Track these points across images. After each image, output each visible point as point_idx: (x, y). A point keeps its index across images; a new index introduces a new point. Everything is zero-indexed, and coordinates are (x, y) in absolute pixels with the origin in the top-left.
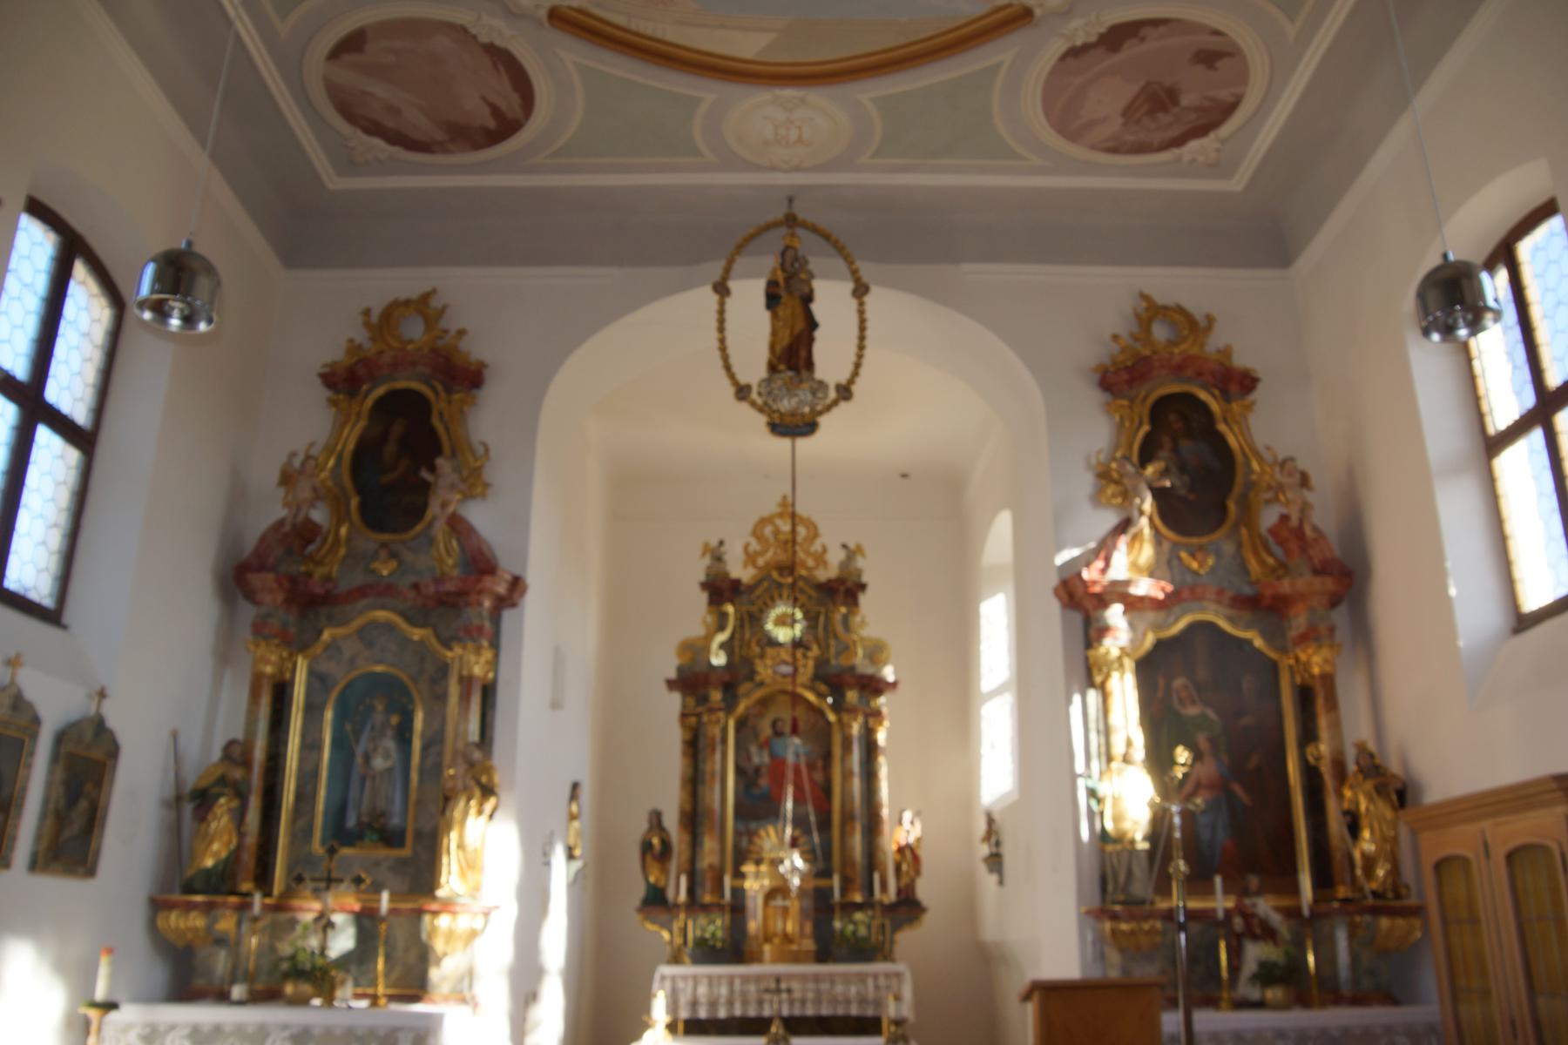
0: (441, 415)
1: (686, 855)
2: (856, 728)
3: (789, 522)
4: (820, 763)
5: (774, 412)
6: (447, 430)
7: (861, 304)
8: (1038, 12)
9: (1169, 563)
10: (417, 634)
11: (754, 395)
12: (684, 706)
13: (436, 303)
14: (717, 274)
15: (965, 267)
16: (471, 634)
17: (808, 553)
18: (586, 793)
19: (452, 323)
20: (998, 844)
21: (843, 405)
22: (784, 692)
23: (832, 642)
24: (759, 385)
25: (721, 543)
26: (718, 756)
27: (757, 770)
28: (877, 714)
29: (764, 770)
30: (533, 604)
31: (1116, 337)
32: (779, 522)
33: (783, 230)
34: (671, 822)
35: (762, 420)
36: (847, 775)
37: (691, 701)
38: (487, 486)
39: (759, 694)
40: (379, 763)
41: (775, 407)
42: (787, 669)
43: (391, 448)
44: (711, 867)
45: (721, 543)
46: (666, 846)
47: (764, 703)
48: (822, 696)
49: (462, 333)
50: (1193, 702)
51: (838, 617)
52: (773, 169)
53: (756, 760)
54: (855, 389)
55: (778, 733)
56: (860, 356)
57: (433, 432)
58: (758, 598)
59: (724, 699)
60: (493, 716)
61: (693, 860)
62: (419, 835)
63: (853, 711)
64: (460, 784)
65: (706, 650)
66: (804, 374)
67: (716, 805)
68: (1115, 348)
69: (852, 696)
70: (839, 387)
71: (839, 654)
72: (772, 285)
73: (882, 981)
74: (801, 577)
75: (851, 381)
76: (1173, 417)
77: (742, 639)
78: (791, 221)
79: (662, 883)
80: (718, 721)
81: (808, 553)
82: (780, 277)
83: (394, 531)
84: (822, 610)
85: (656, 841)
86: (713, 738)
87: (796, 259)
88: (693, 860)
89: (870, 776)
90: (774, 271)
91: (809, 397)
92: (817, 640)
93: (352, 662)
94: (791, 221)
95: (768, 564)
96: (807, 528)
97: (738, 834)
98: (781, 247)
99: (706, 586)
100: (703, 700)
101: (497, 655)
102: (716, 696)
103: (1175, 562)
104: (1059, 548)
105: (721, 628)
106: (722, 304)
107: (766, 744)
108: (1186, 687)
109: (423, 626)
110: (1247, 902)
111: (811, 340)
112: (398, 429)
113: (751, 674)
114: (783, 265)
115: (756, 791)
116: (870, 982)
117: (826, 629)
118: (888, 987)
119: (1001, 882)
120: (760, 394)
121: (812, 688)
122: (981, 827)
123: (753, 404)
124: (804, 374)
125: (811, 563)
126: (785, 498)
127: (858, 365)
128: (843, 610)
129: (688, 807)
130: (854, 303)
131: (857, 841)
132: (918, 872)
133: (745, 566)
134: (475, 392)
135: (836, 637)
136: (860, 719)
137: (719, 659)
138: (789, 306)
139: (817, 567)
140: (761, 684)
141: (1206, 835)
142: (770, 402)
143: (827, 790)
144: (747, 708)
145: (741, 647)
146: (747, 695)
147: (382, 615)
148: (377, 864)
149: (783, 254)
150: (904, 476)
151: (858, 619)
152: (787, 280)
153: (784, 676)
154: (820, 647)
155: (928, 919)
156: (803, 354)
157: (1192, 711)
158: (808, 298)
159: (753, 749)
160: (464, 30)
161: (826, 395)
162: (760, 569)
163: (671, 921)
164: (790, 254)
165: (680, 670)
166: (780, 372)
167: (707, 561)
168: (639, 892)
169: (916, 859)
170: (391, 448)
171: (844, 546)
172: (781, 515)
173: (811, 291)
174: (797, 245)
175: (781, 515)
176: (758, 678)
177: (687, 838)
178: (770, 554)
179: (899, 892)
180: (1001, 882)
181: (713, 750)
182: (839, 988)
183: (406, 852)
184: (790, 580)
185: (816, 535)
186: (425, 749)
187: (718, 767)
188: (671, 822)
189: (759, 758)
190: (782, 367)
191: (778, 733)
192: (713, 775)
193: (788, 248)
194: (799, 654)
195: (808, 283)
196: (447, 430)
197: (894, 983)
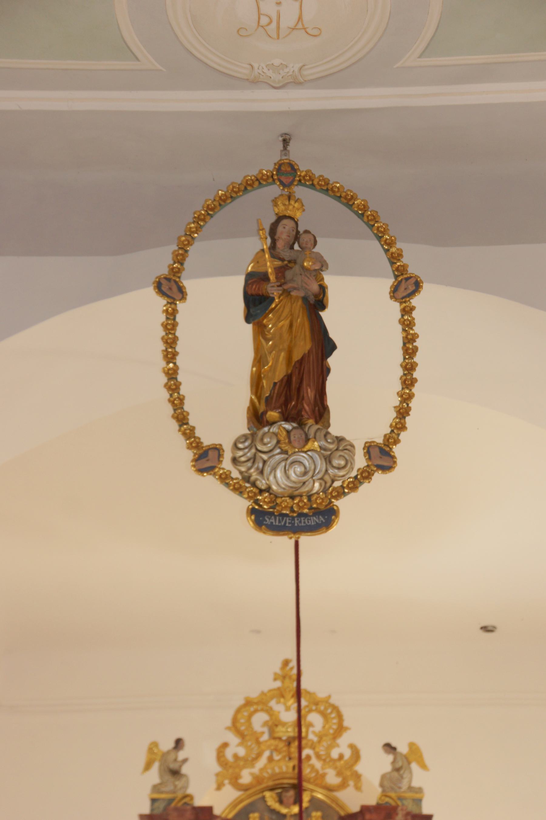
3: (292, 703)
5: (261, 491)
7: (407, 311)
11: (227, 464)
17: (326, 760)
21: (378, 476)
24: (235, 447)
25: (179, 743)
32: (277, 706)
33: (275, 190)
35: (244, 504)
41: (262, 484)
45: (179, 743)
54: (397, 450)
66: (312, 426)
70: (369, 448)
74: (316, 803)
81: (326, 760)
82: (270, 268)
87: (297, 237)
90: (258, 258)
91: (321, 465)
95: (258, 780)
96: (324, 714)
111: (325, 371)
114: (273, 247)
120: (235, 461)
123: (225, 479)
124: (312, 426)
125: (332, 778)
126: (286, 663)
130: (396, 308)
133: (219, 787)
139: (343, 785)
142: (254, 475)
150: (486, 629)
152: (281, 271)
156: (310, 393)
161: (349, 463)
162: (245, 788)
166: (272, 424)
171: (389, 748)
172: (280, 694)
173: (323, 289)
174: (298, 215)
175: (280, 694)
178: (262, 762)
184: (296, 809)
185: (341, 729)
190: (273, 415)
193: (280, 218)
195: (317, 275)
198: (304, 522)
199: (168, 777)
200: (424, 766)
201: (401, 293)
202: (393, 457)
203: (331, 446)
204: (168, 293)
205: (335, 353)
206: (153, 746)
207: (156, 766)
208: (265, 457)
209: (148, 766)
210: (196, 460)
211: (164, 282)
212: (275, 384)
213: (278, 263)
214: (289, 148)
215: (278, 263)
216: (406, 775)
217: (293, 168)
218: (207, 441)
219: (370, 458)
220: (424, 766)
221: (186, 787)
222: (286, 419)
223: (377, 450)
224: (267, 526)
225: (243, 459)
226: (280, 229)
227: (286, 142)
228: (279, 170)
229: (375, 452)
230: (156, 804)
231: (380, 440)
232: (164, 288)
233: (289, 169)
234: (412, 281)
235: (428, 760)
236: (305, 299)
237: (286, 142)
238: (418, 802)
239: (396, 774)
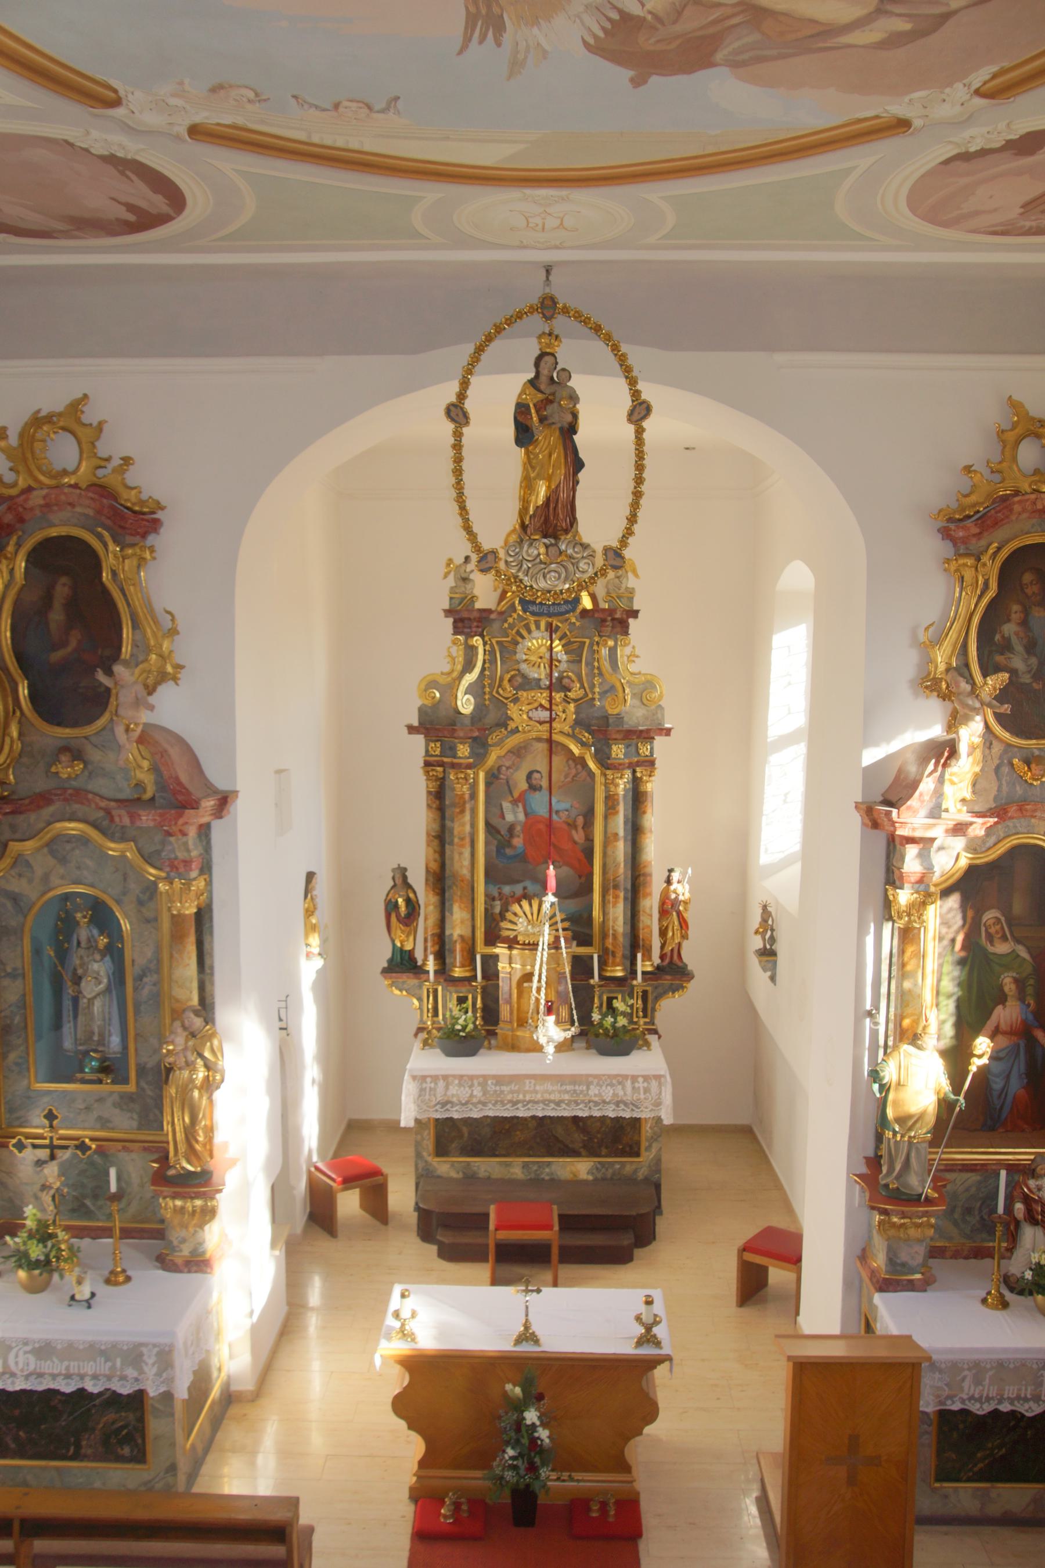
0: (114, 573)
1: (432, 920)
2: (622, 785)
4: (580, 821)
5: (526, 587)
6: (122, 591)
8: (917, 123)
9: (997, 770)
10: (113, 849)
12: (427, 751)
13: (91, 415)
14: (449, 392)
15: (780, 358)
16: (176, 868)
18: (322, 888)
19: (112, 446)
20: (773, 939)
22: (539, 740)
23: (597, 680)
26: (467, 817)
27: (511, 829)
28: (650, 763)
29: (518, 828)
30: (242, 808)
31: (968, 469)
34: (418, 879)
36: (609, 840)
37: (436, 748)
38: (179, 667)
39: (513, 741)
40: (89, 988)
42: (545, 715)
43: (57, 616)
44: (461, 937)
46: (413, 906)
47: (519, 752)
48: (583, 744)
49: (127, 461)
50: (1004, 938)
51: (604, 652)
52: (523, 247)
53: (509, 817)
55: (533, 788)
56: (635, 505)
57: (105, 592)
58: (511, 626)
59: (473, 754)
60: (212, 942)
61: (442, 923)
62: (141, 1071)
63: (617, 767)
64: (181, 1061)
65: (452, 690)
67: (465, 872)
68: (964, 484)
69: (618, 751)
70: (607, 550)
71: (603, 694)
72: (521, 409)
73: (641, 1084)
75: (624, 541)
76: (1027, 577)
77: (492, 678)
78: (548, 307)
79: (408, 947)
80: (466, 779)
83: (75, 725)
84: (587, 641)
85: (400, 900)
86: (463, 794)
88: (442, 923)
89: (636, 831)
92: (580, 680)
93: (46, 878)
94: (548, 307)
97: (490, 898)
98: (537, 352)
99: (448, 613)
100: (452, 751)
101: (209, 883)
102: (464, 750)
103: (1006, 769)
104: (868, 741)
105: (468, 666)
106: (458, 435)
107: (520, 800)
108: (998, 920)
109: (123, 839)
110: (1032, 1183)
112: (62, 589)
113: (503, 722)
115: (509, 852)
116: (629, 1083)
117: (587, 664)
118: (647, 1090)
119: (773, 978)
121: (573, 736)
122: (755, 919)
127: (632, 519)
128: (611, 643)
129: (434, 866)
130: (632, 428)
131: (618, 913)
132: (685, 937)
134: (151, 539)
135: (601, 674)
136: (628, 774)
137: (466, 704)
138: (547, 439)
140: (516, 731)
141: (997, 1085)
143: (589, 853)
144: (499, 757)
145: (491, 686)
146: (499, 743)
147: (73, 828)
148: (100, 1100)
149: (537, 363)
151: (628, 650)
153: (541, 723)
154: (582, 687)
155: (691, 985)
157: (1002, 948)
158: (571, 429)
159: (506, 805)
160: (72, 145)
163: (420, 987)
164: (547, 362)
165: (421, 711)
167: (451, 581)
168: (385, 953)
169: (683, 924)
170: (57, 616)
176: (512, 725)
177: (434, 899)
179: (662, 957)
180: (773, 978)
181: (463, 811)
182: (594, 1091)
183: (131, 1087)
186: (139, 978)
187: (468, 828)
188: (418, 879)
189: (514, 815)
191: (533, 788)
192: (462, 839)
194: (558, 696)
196: (122, 591)
197: (654, 1084)
198: (557, 609)
199: (460, 583)
200: (637, 576)
201: (636, 417)
202: (623, 558)
203: (578, 556)
204: (455, 418)
205: (583, 471)
206: (450, 561)
207: (452, 573)
208: (530, 565)
209: (446, 576)
210: (479, 562)
211: (452, 408)
212: (538, 507)
213: (540, 396)
214: (551, 278)
215: (540, 396)
216: (624, 581)
217: (553, 300)
218: (486, 546)
219: (605, 560)
220: (637, 576)
221: (473, 589)
222: (545, 536)
223: (612, 552)
224: (530, 612)
225: (513, 564)
226: (542, 364)
227: (548, 272)
228: (542, 303)
229: (611, 554)
230: (453, 601)
231: (615, 544)
232: (453, 414)
233: (550, 303)
234: (644, 406)
235: (639, 572)
236: (561, 429)
237: (548, 272)
238: (631, 599)
239: (617, 580)
